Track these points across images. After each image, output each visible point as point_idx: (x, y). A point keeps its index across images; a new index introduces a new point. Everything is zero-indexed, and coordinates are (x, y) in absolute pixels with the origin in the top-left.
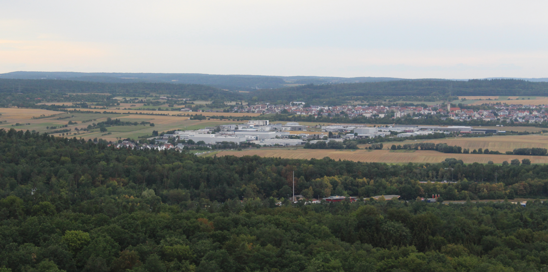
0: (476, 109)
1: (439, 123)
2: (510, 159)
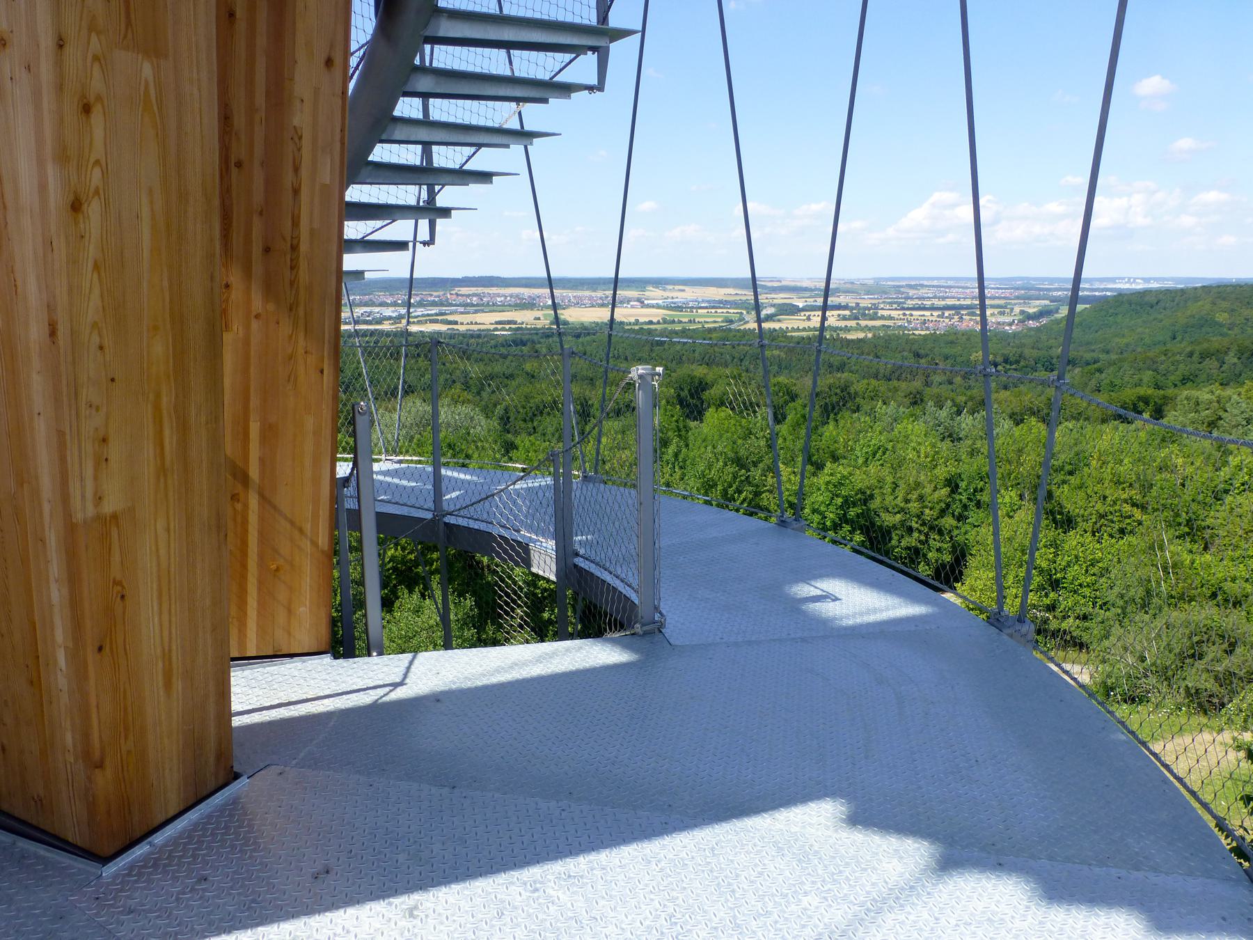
0: (468, 296)
1: (442, 305)
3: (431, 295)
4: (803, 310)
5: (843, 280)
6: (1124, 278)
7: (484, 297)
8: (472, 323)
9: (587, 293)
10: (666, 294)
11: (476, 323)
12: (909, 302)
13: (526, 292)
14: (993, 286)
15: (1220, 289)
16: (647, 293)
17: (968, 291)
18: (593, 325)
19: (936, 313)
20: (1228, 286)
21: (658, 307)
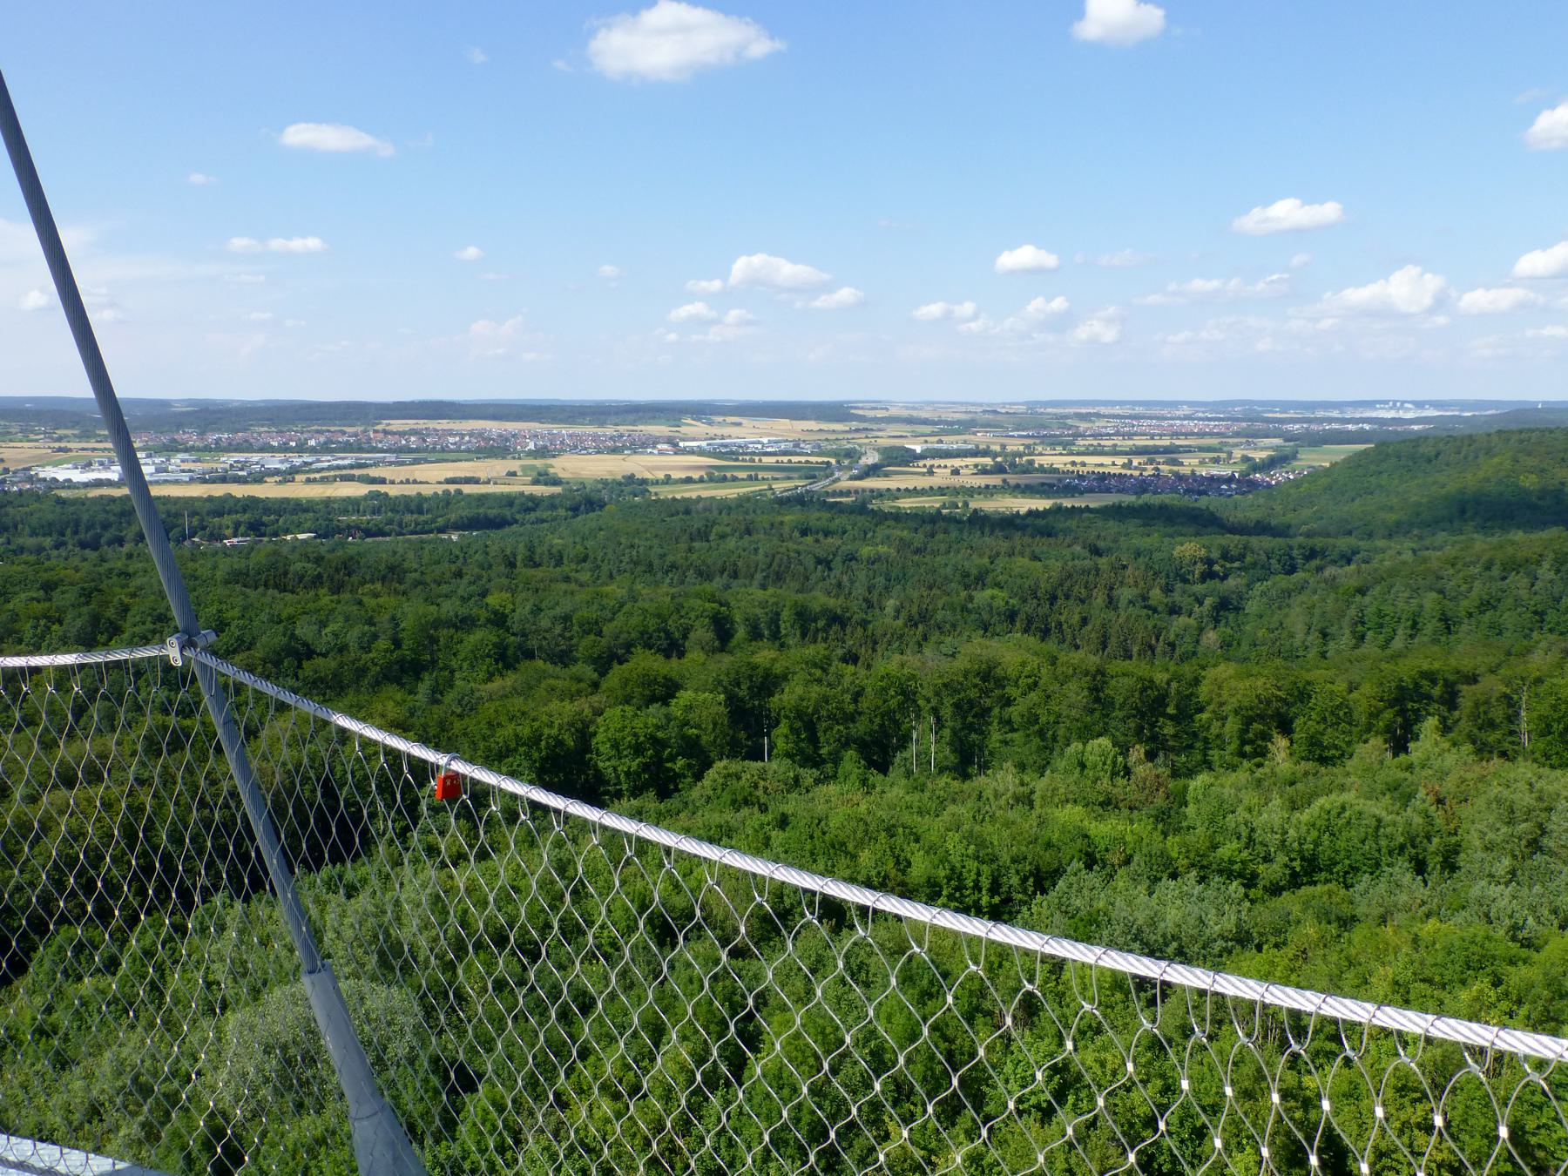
0: (402, 434)
1: (361, 450)
2: (440, 489)
3: (344, 433)
4: (922, 457)
5: (981, 405)
6: (1386, 402)
7: (428, 435)
8: (408, 482)
9: (591, 430)
10: (713, 430)
11: (415, 482)
12: (1080, 442)
13: (493, 427)
14: (1200, 415)
15: (1523, 436)
16: (683, 429)
17: (1165, 423)
18: (600, 486)
19: (1120, 461)
20: (1533, 431)
21: (700, 452)
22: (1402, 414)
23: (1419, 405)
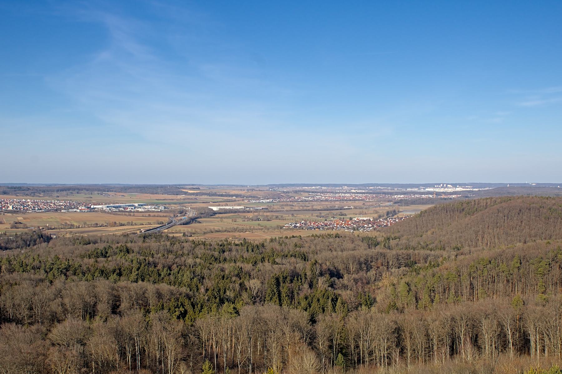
6: (440, 184)
14: (353, 191)
17: (337, 195)
22: (446, 190)
23: (455, 185)
